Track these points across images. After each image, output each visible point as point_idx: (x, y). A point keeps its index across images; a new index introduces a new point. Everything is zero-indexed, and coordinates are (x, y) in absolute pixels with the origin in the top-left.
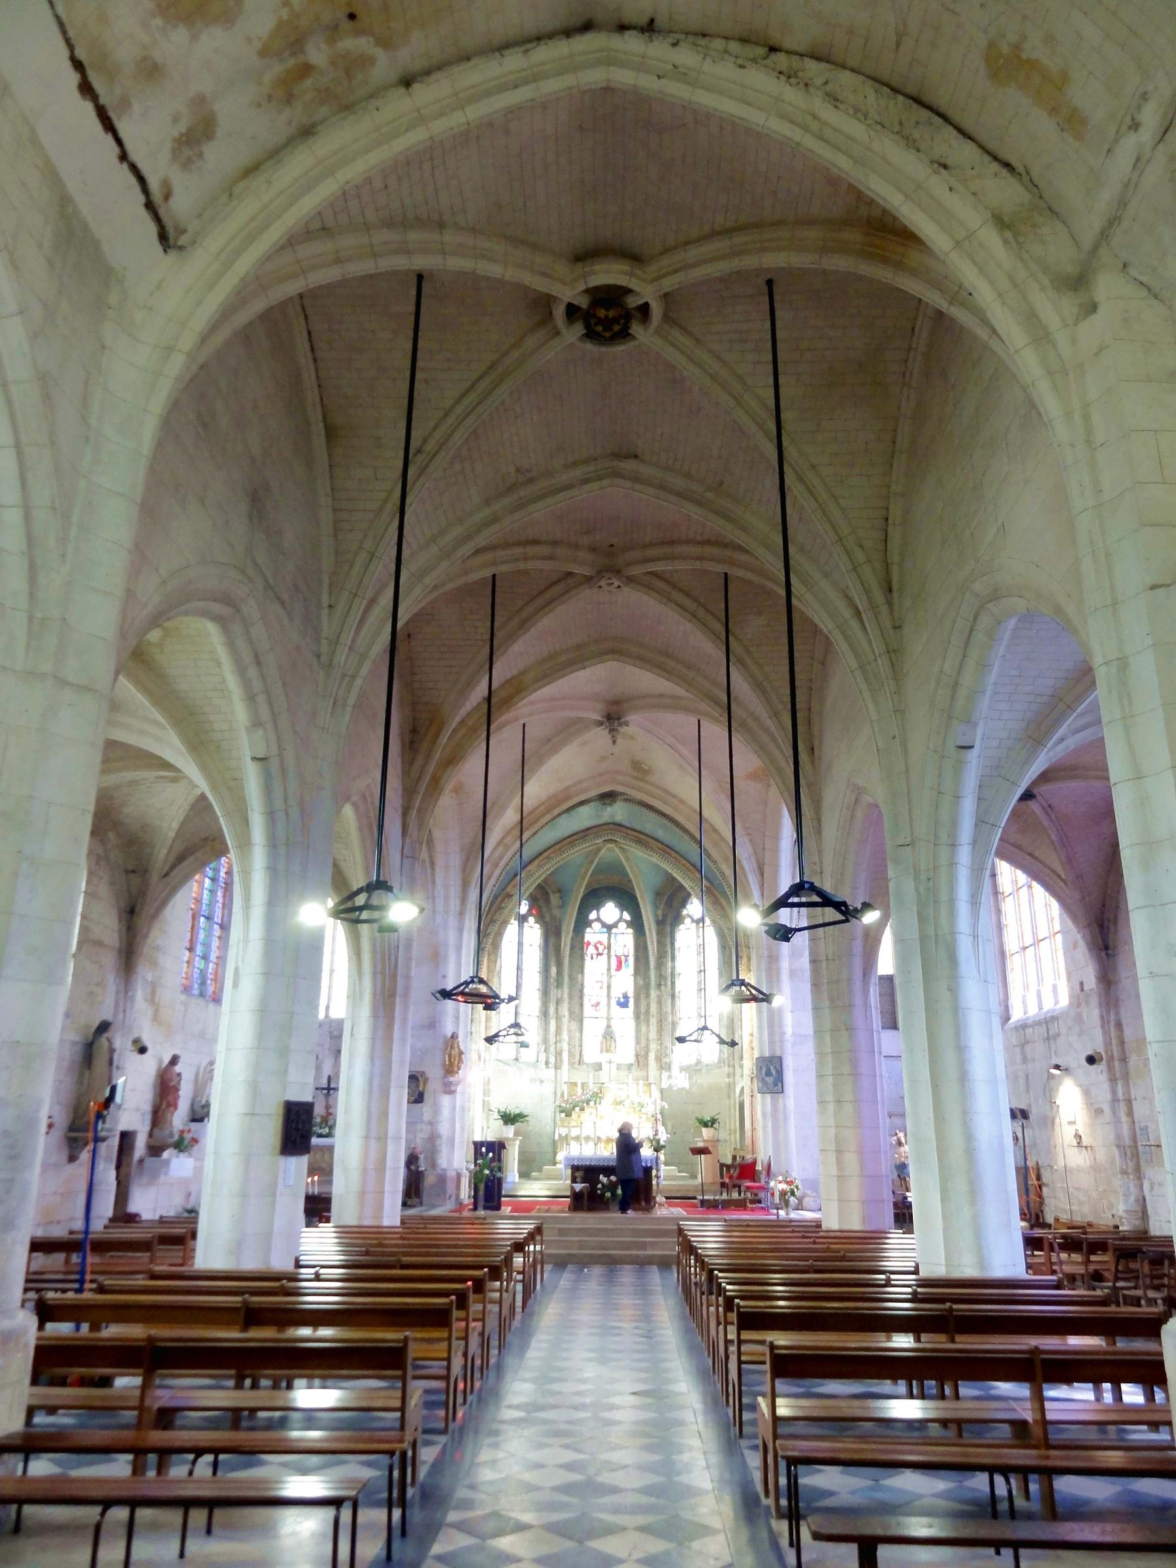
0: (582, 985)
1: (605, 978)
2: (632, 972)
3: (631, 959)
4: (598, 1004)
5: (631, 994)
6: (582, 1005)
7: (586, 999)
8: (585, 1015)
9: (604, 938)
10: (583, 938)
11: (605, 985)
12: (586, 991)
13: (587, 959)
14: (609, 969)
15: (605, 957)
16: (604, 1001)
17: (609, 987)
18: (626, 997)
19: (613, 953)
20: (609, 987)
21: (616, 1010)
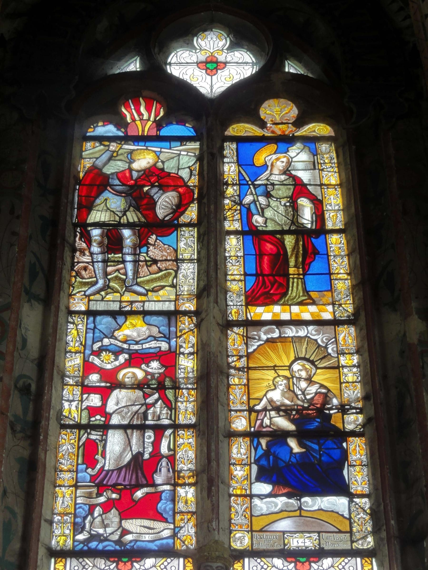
0: (46, 364)
1: (188, 342)
2: (348, 308)
3: (337, 243)
4: (142, 468)
5: (353, 421)
6: (33, 475)
7: (67, 445)
8: (61, 536)
9: (182, 160)
10: (65, 149)
11: (187, 365)
12: (72, 405)
13: (89, 257)
14: (211, 283)
15: (187, 243)
16: (187, 449)
17: (212, 377)
18: (315, 423)
19: (232, 224)
20: (212, 377)
21: (261, 505)
